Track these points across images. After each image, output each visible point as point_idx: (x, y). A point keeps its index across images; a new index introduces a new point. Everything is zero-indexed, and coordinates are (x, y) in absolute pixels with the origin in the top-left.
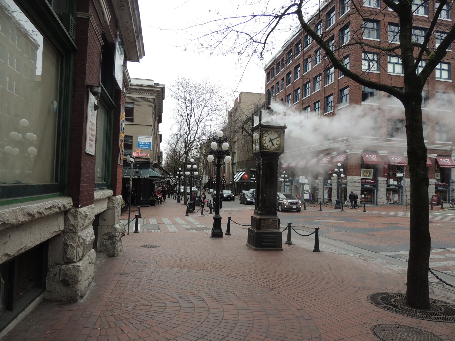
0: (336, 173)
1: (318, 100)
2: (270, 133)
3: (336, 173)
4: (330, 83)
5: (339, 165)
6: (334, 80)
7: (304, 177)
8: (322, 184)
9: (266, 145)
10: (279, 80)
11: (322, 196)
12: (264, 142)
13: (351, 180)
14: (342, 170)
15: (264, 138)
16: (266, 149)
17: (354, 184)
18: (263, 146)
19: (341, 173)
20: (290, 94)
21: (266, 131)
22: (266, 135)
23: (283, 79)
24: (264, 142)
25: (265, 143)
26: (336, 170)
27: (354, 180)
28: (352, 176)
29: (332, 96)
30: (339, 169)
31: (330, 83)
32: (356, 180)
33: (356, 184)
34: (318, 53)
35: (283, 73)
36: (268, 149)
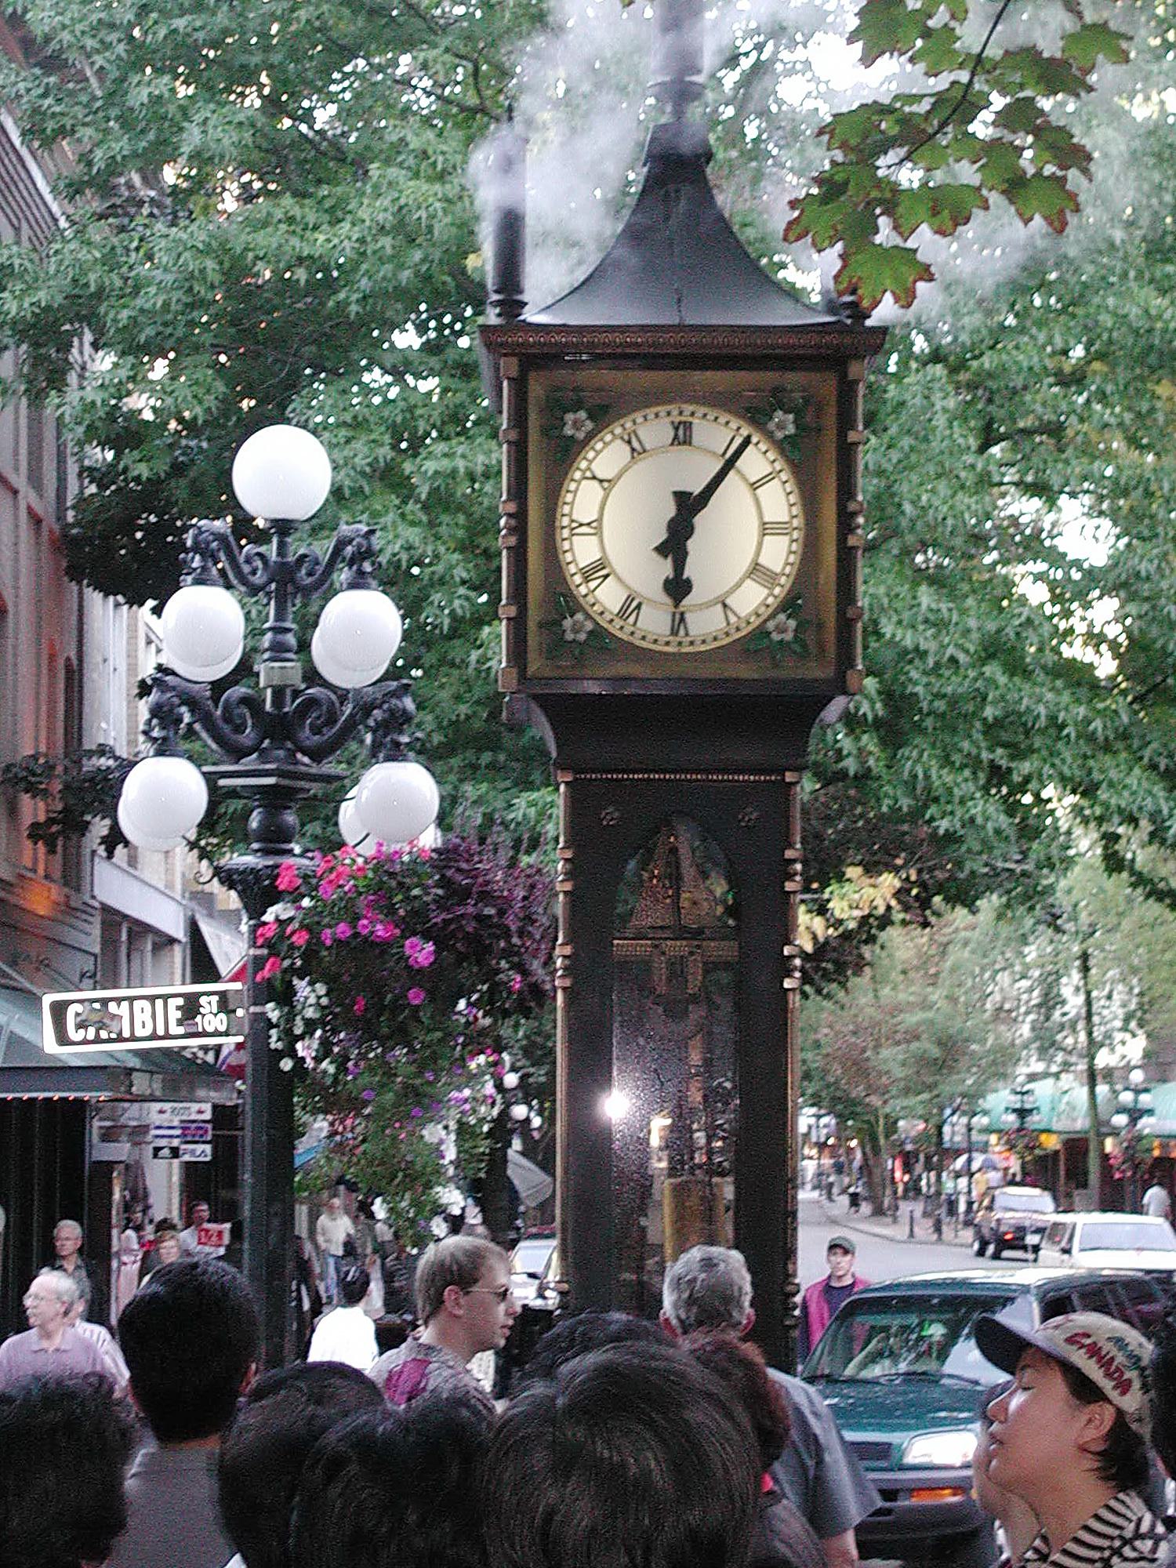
15: (582, 500)
22: (606, 456)
25: (599, 569)
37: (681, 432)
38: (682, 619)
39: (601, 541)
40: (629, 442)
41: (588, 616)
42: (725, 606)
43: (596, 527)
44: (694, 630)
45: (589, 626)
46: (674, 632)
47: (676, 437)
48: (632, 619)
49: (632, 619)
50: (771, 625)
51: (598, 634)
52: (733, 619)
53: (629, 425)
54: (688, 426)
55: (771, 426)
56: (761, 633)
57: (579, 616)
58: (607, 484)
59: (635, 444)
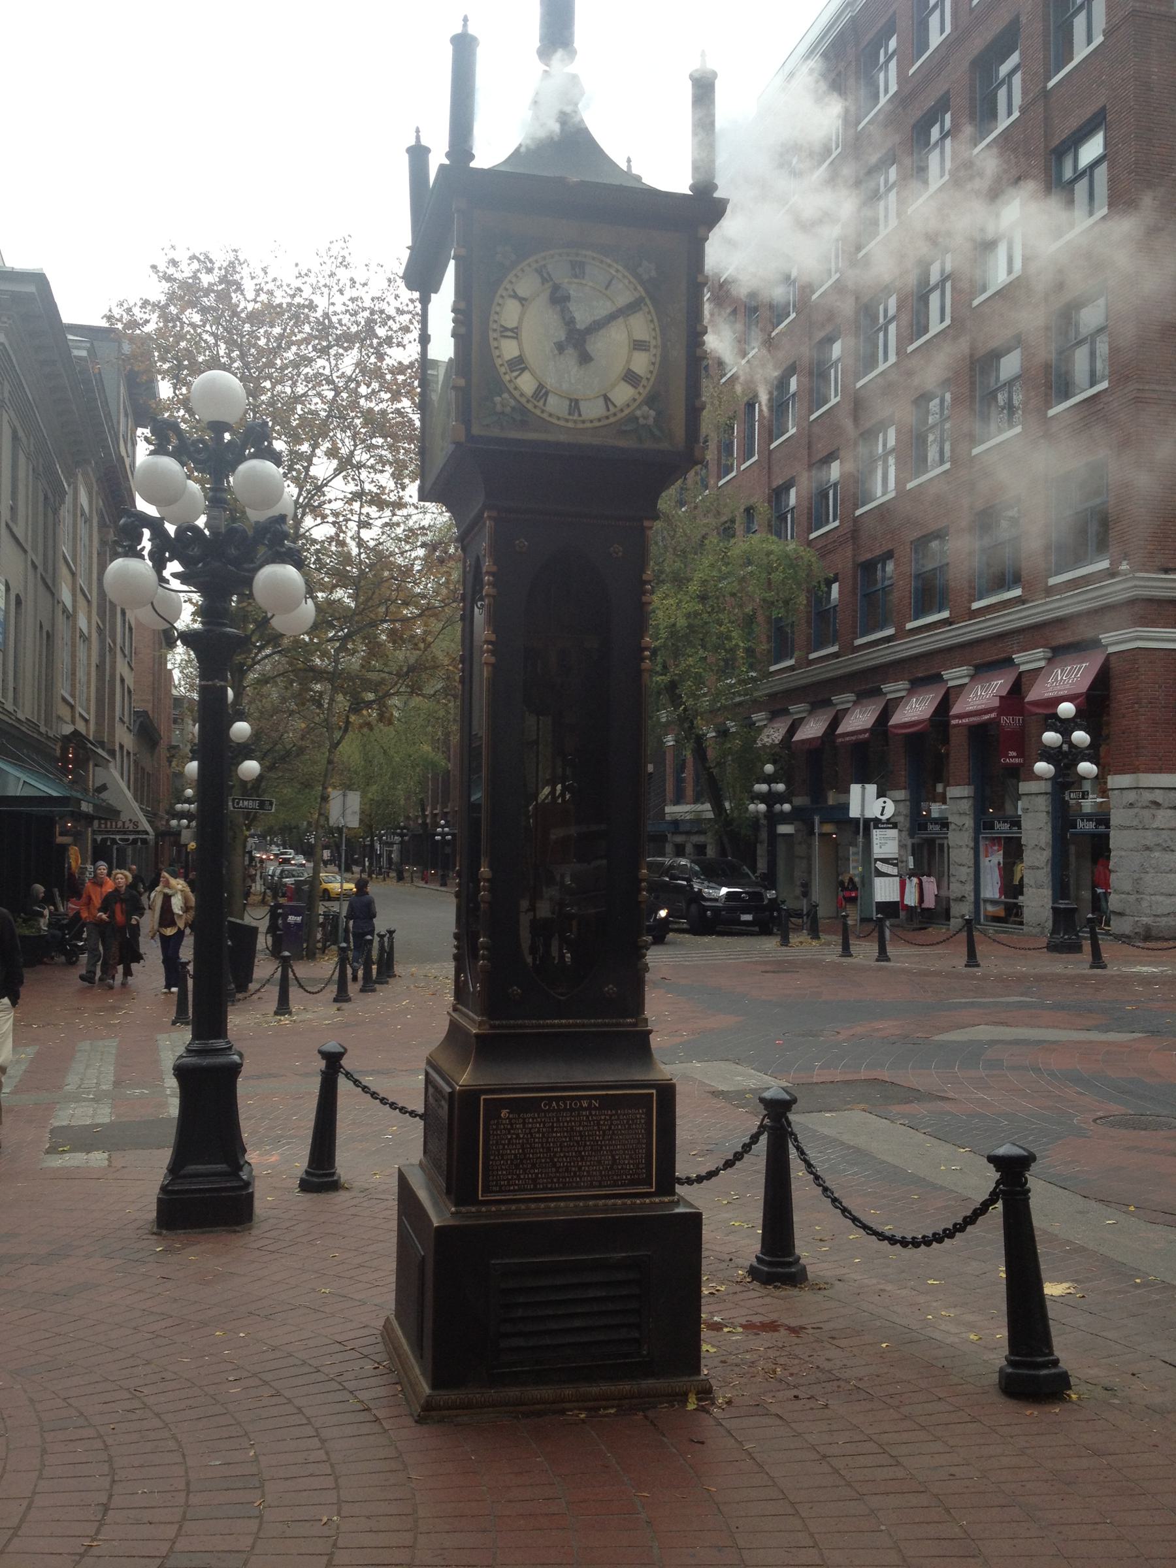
0: (1048, 754)
3: (1048, 754)
5: (1067, 709)
7: (872, 789)
8: (969, 822)
9: (526, 384)
11: (969, 887)
13: (1131, 796)
14: (1080, 737)
15: (510, 313)
16: (522, 415)
17: (1146, 813)
18: (498, 386)
19: (1078, 754)
24: (509, 349)
25: (519, 364)
26: (1051, 737)
27: (1148, 796)
28: (1135, 770)
30: (1066, 732)
32: (1158, 796)
33: (1161, 813)
34: (935, 133)
39: (520, 345)
42: (607, 399)
43: (515, 333)
49: (542, 402)
50: (638, 413)
51: (522, 410)
54: (582, 265)
56: (633, 419)
57: (506, 395)
58: (522, 301)
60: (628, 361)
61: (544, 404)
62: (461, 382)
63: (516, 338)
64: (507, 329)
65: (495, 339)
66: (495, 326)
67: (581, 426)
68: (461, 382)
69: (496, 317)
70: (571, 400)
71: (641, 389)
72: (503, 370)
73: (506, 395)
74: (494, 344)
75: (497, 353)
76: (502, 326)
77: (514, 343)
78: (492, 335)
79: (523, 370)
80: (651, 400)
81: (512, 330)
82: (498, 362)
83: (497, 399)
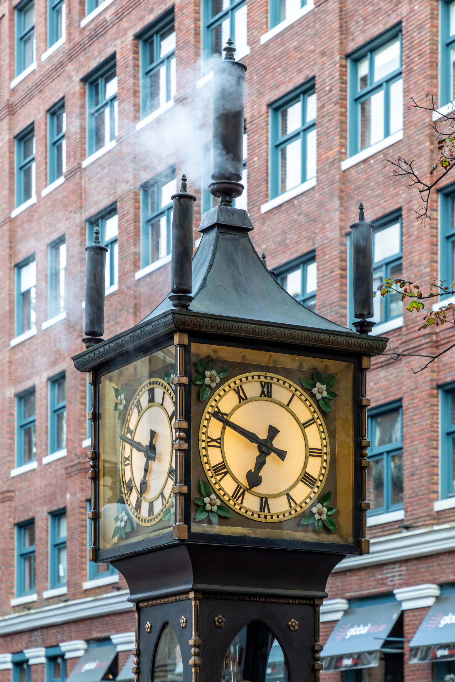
1: (304, 248)
2: (252, 389)
4: (377, 141)
6: (407, 125)
10: (34, 112)
12: (214, 456)
18: (208, 489)
20: (111, 211)
21: (229, 370)
23: (56, 111)
29: (395, 229)
31: (377, 141)
35: (57, 68)
36: (243, 520)
37: (265, 389)
38: (266, 503)
40: (238, 393)
41: (218, 497)
43: (219, 443)
44: (274, 510)
45: (219, 503)
46: (262, 510)
47: (263, 392)
48: (239, 501)
49: (239, 501)
52: (293, 505)
53: (238, 382)
54: (269, 385)
55: (315, 390)
57: (213, 496)
59: (241, 394)
60: (305, 466)
61: (242, 503)
62: (185, 489)
63: (220, 447)
64: (213, 440)
65: (204, 448)
66: (203, 437)
67: (269, 519)
68: (185, 489)
69: (204, 430)
70: (262, 498)
71: (316, 490)
72: (210, 474)
73: (213, 496)
74: (204, 452)
75: (205, 460)
76: (209, 437)
77: (219, 449)
78: (203, 445)
79: (225, 473)
80: (325, 497)
81: (216, 441)
82: (207, 467)
83: (207, 500)
